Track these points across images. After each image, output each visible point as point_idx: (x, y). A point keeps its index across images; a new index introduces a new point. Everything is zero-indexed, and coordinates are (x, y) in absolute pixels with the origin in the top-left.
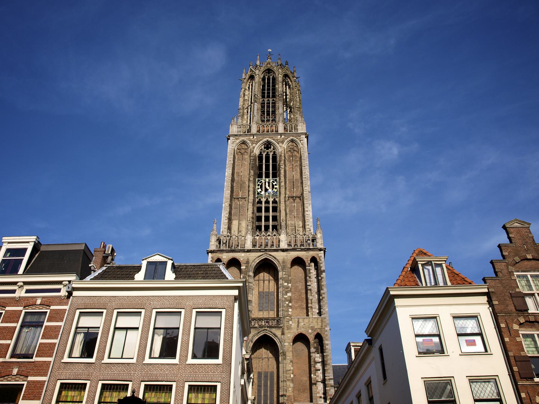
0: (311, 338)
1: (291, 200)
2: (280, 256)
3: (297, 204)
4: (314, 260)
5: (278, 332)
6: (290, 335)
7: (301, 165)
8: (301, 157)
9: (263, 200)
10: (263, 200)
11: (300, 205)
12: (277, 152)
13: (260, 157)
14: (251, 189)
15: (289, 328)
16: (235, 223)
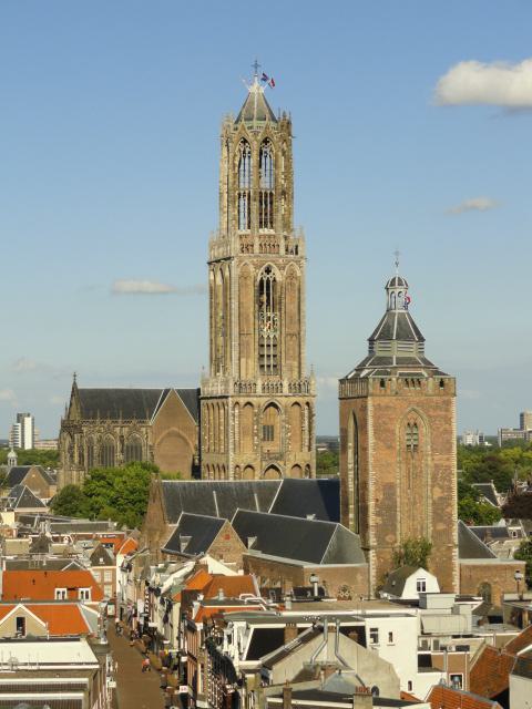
0: (303, 466)
1: (289, 337)
2: (284, 400)
3: (293, 343)
4: (308, 404)
5: (282, 463)
6: (290, 466)
7: (299, 298)
8: (299, 290)
9: (265, 336)
10: (265, 336)
11: (297, 343)
12: (277, 279)
13: (262, 281)
14: (257, 327)
15: (289, 460)
16: (243, 360)
